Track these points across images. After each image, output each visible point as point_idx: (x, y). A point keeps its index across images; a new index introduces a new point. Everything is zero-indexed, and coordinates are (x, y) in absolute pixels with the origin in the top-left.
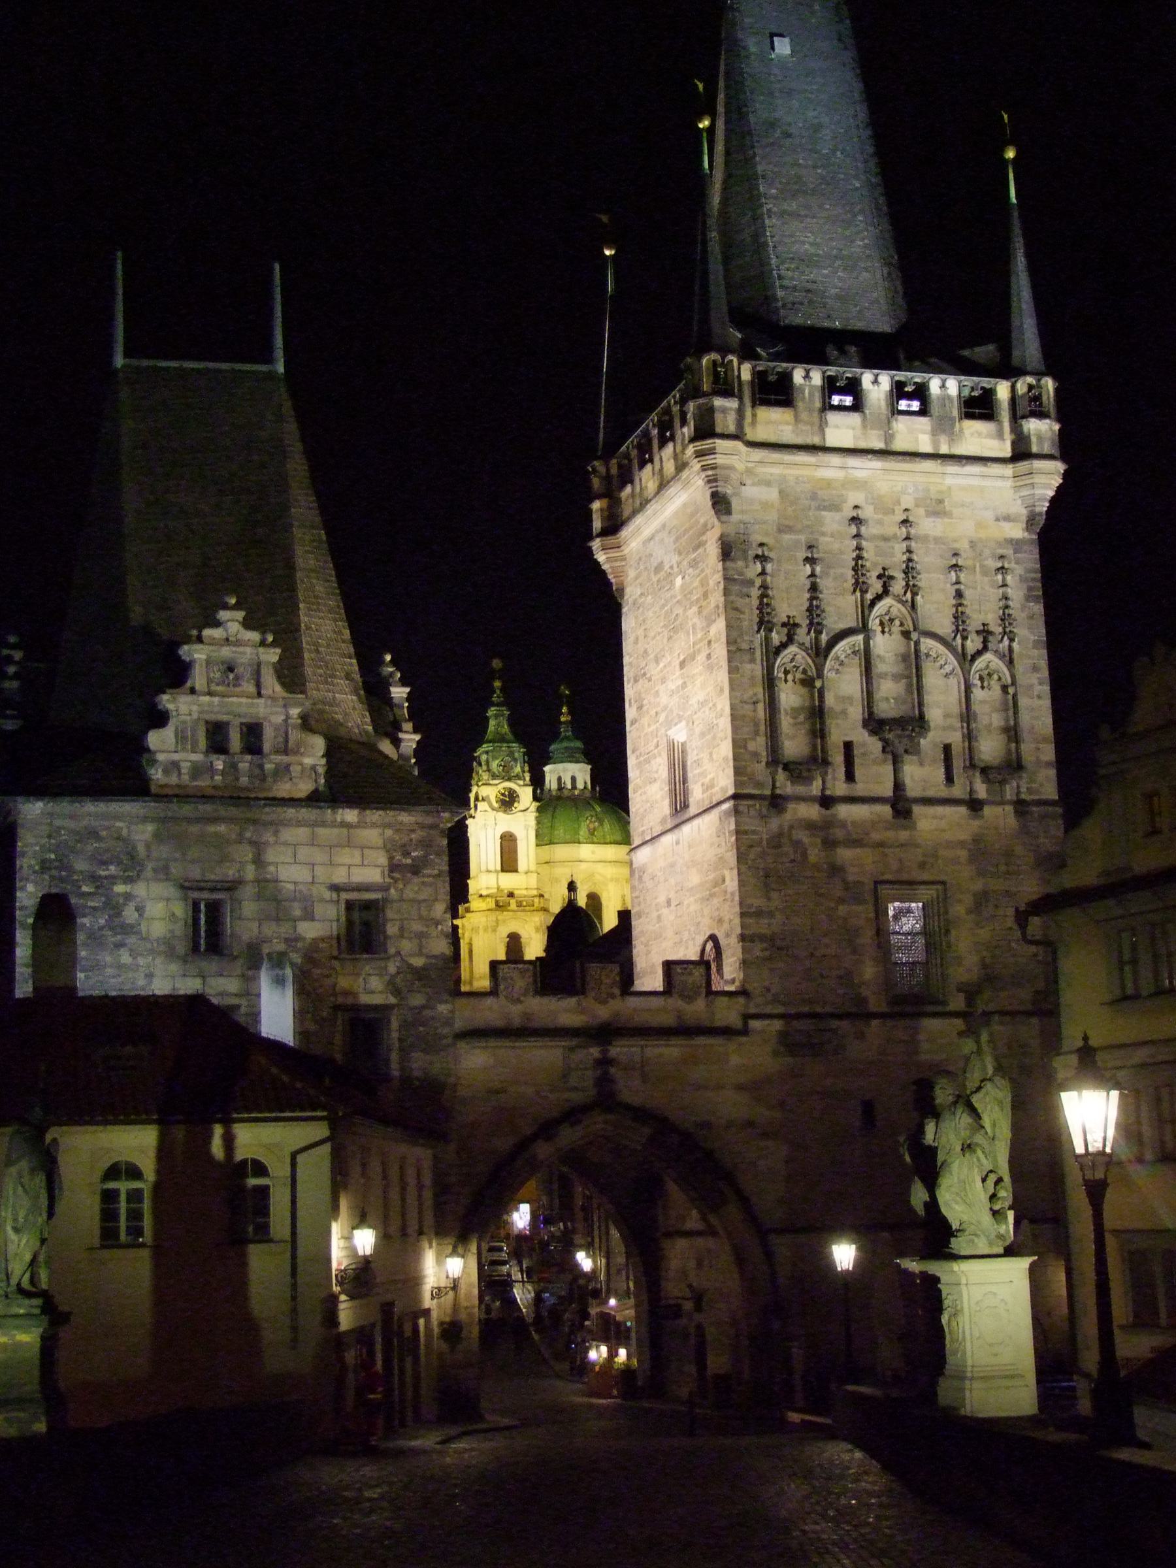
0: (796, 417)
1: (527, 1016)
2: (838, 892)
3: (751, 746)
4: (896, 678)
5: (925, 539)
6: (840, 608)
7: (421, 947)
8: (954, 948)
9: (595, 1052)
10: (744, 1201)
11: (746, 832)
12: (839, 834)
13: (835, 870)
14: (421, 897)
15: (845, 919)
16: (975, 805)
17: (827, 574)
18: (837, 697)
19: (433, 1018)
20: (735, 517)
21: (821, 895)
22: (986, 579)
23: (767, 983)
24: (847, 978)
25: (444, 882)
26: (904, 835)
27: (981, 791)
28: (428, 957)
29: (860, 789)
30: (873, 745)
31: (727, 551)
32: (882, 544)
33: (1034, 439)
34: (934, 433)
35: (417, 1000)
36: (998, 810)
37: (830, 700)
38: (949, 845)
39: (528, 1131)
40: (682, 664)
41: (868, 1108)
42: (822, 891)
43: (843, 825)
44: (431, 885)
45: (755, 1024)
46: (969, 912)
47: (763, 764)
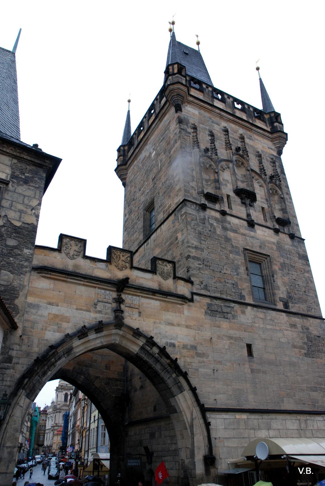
0: (204, 95)
1: (76, 266)
2: (229, 249)
3: (191, 184)
4: (243, 182)
5: (248, 144)
6: (223, 153)
7: (20, 217)
8: (276, 282)
9: (114, 295)
10: (193, 390)
11: (190, 214)
12: (228, 226)
13: (228, 240)
14: (26, 193)
15: (233, 260)
16: (277, 231)
17: (217, 142)
18: (223, 180)
19: (19, 255)
20: (183, 113)
21: (222, 247)
22: (268, 163)
23: (201, 280)
24: (235, 285)
25: (40, 192)
26: (252, 234)
27: (277, 227)
28: (24, 223)
29: (234, 212)
30: (238, 200)
31: (180, 121)
32: (234, 140)
33: (278, 127)
34: (247, 117)
35: (11, 242)
36: (284, 235)
37: (221, 179)
38: (269, 242)
39: (70, 331)
40: (153, 180)
41: (249, 347)
42: (223, 246)
43: (230, 224)
44: (33, 190)
45: (195, 297)
46: (280, 269)
47: (196, 191)
